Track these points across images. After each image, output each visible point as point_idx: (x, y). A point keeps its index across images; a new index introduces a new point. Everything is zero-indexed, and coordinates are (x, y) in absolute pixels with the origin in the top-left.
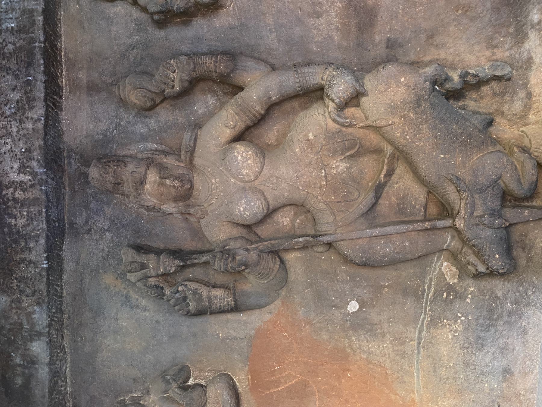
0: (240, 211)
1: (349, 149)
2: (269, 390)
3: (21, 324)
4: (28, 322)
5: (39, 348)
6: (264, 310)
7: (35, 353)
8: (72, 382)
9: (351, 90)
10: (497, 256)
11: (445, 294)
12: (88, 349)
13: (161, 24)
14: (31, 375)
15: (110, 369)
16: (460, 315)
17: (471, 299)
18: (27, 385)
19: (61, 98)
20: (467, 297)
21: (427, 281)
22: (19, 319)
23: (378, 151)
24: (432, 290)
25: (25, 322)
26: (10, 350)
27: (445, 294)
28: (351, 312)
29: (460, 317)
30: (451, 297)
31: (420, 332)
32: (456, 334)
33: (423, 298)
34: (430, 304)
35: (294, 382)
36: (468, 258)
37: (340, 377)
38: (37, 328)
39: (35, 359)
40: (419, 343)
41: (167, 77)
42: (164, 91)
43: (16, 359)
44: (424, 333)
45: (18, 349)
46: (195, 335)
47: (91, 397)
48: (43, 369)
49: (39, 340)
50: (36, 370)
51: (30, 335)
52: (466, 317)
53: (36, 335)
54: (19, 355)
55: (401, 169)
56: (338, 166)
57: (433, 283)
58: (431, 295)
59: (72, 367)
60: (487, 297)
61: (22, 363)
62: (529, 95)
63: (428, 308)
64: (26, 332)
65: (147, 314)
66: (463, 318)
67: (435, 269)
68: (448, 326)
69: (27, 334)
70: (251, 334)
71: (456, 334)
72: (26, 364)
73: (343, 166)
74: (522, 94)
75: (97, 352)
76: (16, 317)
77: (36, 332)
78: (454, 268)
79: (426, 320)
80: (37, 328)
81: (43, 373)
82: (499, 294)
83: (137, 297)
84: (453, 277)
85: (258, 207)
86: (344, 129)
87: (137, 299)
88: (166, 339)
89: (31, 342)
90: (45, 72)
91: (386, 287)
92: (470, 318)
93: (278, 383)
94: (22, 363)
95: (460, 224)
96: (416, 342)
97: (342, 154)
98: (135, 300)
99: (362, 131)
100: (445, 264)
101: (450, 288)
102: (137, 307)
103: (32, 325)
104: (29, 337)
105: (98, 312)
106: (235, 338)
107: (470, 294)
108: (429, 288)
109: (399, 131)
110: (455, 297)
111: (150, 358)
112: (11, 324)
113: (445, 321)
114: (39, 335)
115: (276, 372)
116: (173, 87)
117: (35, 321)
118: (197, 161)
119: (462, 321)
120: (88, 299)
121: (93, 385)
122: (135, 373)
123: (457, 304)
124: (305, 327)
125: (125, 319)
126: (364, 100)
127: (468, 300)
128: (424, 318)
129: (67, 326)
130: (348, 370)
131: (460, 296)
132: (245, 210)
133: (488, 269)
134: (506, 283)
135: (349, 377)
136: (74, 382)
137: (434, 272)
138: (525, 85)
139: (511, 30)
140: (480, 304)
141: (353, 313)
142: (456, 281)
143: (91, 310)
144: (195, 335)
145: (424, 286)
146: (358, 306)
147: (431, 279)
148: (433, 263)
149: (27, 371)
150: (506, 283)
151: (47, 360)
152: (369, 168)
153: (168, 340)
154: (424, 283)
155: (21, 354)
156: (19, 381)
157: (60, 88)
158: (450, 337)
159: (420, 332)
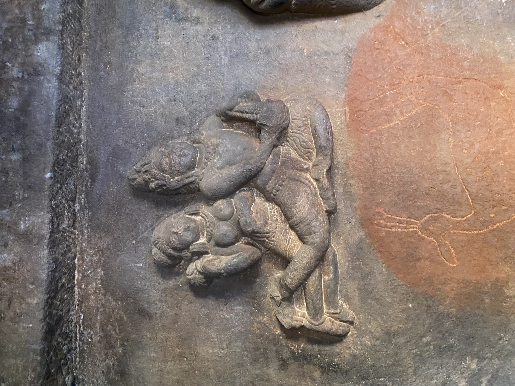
2: (376, 127)
3: (23, 21)
4: (33, 15)
5: (45, 52)
6: (368, 12)
7: (40, 60)
8: (88, 127)
12: (114, 79)
14: (32, 93)
15: (143, 107)
18: (25, 109)
22: (21, 13)
25: (29, 16)
26: (5, 58)
35: (414, 112)
37: (486, 98)
38: (46, 23)
39: (40, 68)
43: (12, 70)
45: (16, 55)
46: (268, 52)
47: (114, 149)
48: (49, 82)
49: (48, 40)
50: (40, 84)
51: (35, 35)
53: (43, 34)
54: (17, 65)
59: (89, 106)
61: (20, 75)
64: (29, 30)
65: (199, 28)
69: (30, 33)
70: (350, 46)
72: (26, 77)
75: (127, 84)
76: (17, 11)
77: (45, 28)
80: (46, 23)
81: (50, 87)
83: (186, 5)
87: (187, 9)
88: (225, 60)
89: (37, 44)
93: (389, 115)
94: (20, 75)
98: (183, 11)
102: (186, 19)
103: (39, 19)
104: (33, 38)
105: (130, 29)
106: (326, 53)
111: (201, 87)
112: (10, 21)
114: (48, 32)
115: (388, 100)
117: (44, 14)
120: (118, 10)
121: (117, 131)
122: (179, 110)
124: (433, 29)
125: (168, 37)
129: (87, 48)
130: (500, 87)
135: (502, 97)
136: (91, 126)
143: (121, 26)
144: (268, 52)
149: (26, 88)
151: (58, 70)
153: (229, 61)
155: (20, 64)
156: (14, 103)
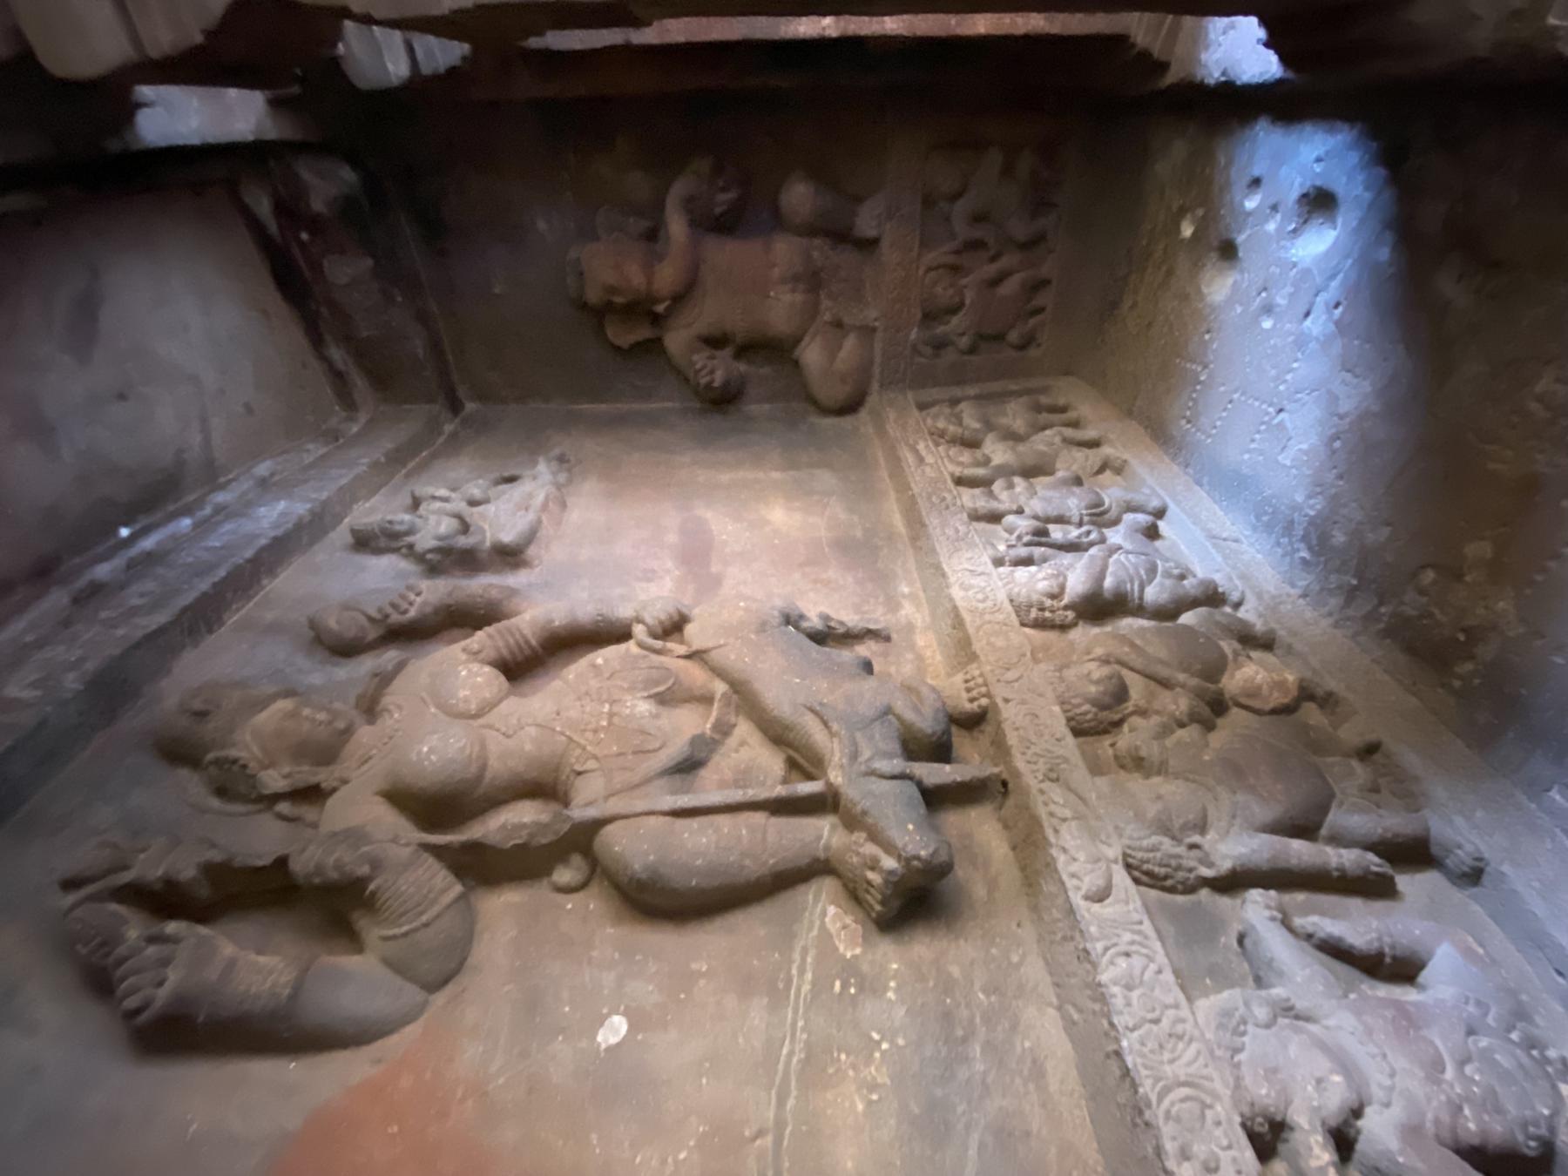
0: (420, 752)
1: (657, 683)
9: (672, 610)
10: (911, 827)
11: (838, 984)
13: (433, 570)
16: (876, 1036)
17: (897, 990)
19: (210, 631)
20: (886, 989)
21: (797, 956)
23: (706, 700)
24: (809, 976)
27: (838, 984)
28: (603, 1046)
29: (879, 1043)
30: (852, 991)
31: (781, 1102)
32: (875, 1097)
33: (788, 997)
34: (806, 1012)
36: (861, 850)
40: (778, 1141)
41: (403, 597)
42: (387, 616)
44: (791, 1103)
52: (892, 1042)
55: (744, 729)
56: (634, 706)
57: (809, 960)
58: (806, 988)
60: (931, 984)
62: (920, 658)
63: (800, 1024)
66: (885, 1046)
67: (812, 923)
68: (851, 1073)
71: (875, 1097)
73: (644, 707)
74: (910, 656)
78: (848, 920)
79: (795, 1060)
82: (955, 971)
84: (851, 943)
85: (463, 749)
86: (655, 658)
90: (215, 585)
91: (701, 975)
92: (901, 1042)
95: (836, 777)
96: (769, 1140)
97: (645, 689)
99: (682, 662)
100: (832, 910)
101: (849, 970)
107: (894, 978)
108: (802, 972)
109: (734, 656)
110: (861, 989)
113: (843, 1057)
116: (405, 612)
118: (387, 700)
119: (883, 1053)
123: (869, 1008)
126: (689, 629)
127: (891, 995)
128: (791, 1053)
131: (870, 986)
132: (431, 751)
133: (899, 858)
134: (962, 942)
137: (810, 929)
138: (912, 647)
139: (881, 599)
140: (920, 1001)
141: (609, 1049)
142: (858, 951)
145: (790, 969)
146: (624, 1028)
147: (805, 951)
148: (805, 909)
150: (962, 942)
152: (687, 724)
154: (791, 962)
157: (220, 622)
158: (860, 1107)
159: (781, 1102)
